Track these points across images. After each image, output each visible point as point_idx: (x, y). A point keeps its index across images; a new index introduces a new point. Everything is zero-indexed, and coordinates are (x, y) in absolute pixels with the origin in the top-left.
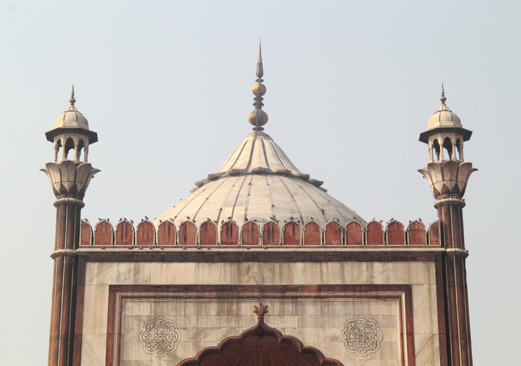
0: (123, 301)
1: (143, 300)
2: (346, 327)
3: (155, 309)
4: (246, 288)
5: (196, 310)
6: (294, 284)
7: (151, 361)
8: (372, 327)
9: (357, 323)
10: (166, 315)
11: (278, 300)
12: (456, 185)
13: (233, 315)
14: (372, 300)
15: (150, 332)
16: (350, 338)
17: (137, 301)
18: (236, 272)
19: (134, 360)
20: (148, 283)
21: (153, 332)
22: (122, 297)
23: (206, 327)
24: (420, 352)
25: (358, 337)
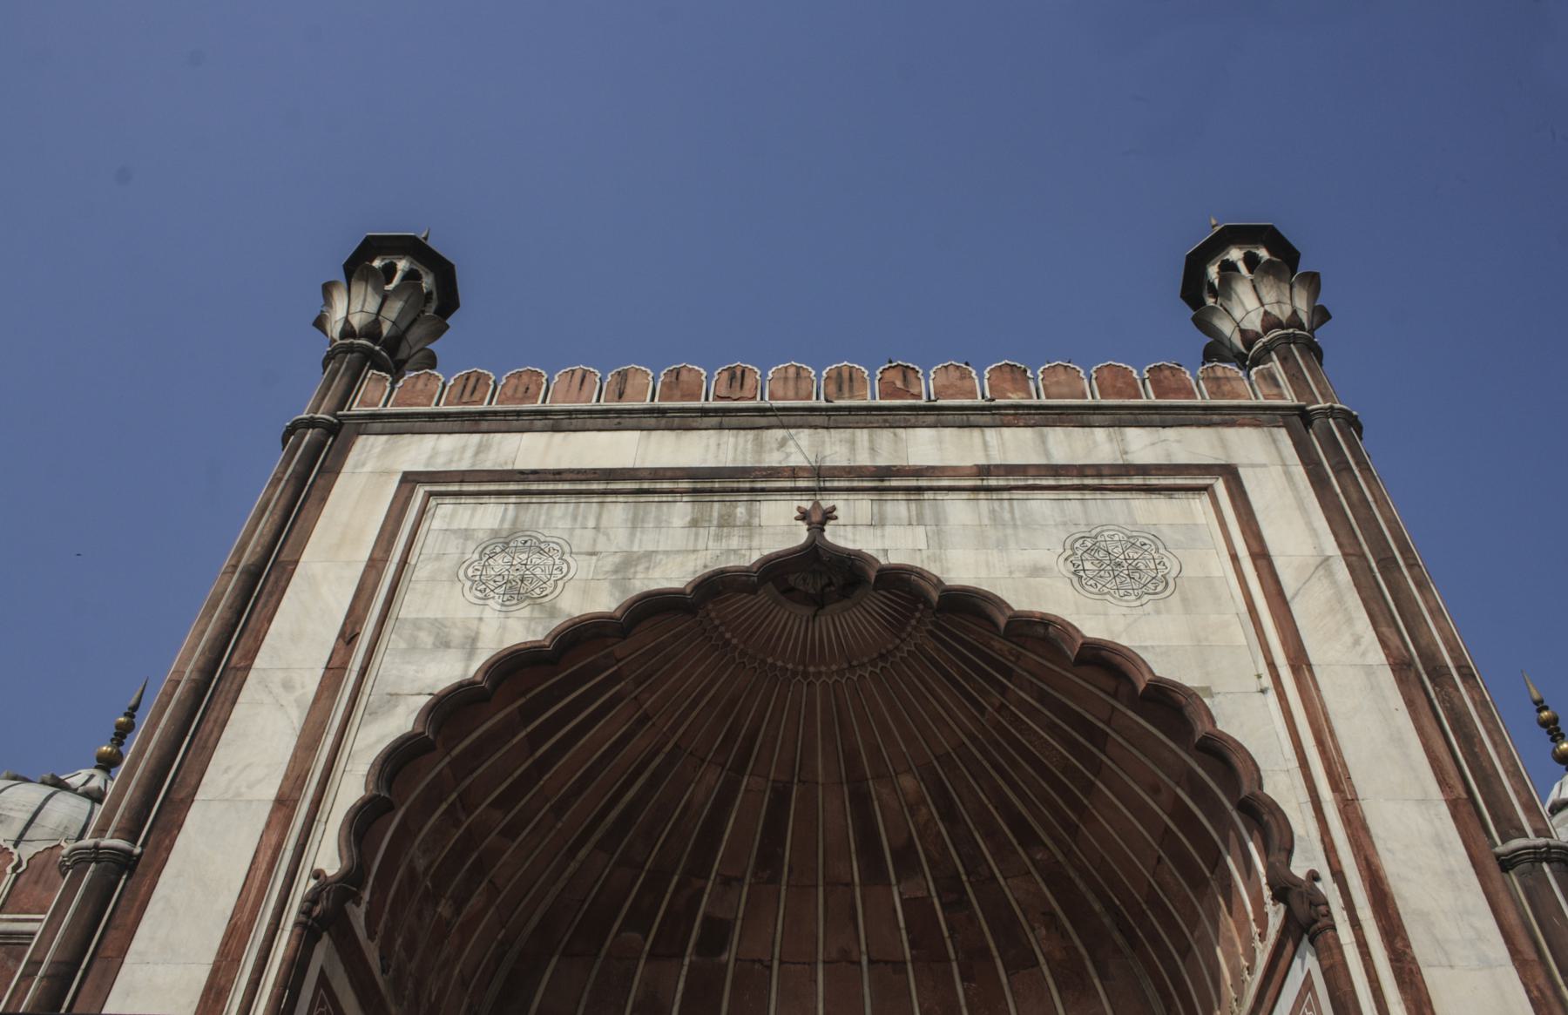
0: (433, 502)
1: (485, 499)
2: (1068, 543)
3: (516, 518)
4: (773, 473)
5: (630, 516)
6: (911, 463)
7: (481, 619)
8: (1145, 547)
9: (1099, 539)
10: (544, 528)
11: (865, 497)
12: (1295, 312)
13: (734, 526)
14: (1135, 495)
15: (491, 561)
16: (1084, 570)
17: (468, 501)
18: (749, 446)
19: (428, 618)
20: (509, 467)
21: (500, 562)
22: (431, 494)
23: (655, 549)
24: (1301, 592)
25: (1109, 568)
